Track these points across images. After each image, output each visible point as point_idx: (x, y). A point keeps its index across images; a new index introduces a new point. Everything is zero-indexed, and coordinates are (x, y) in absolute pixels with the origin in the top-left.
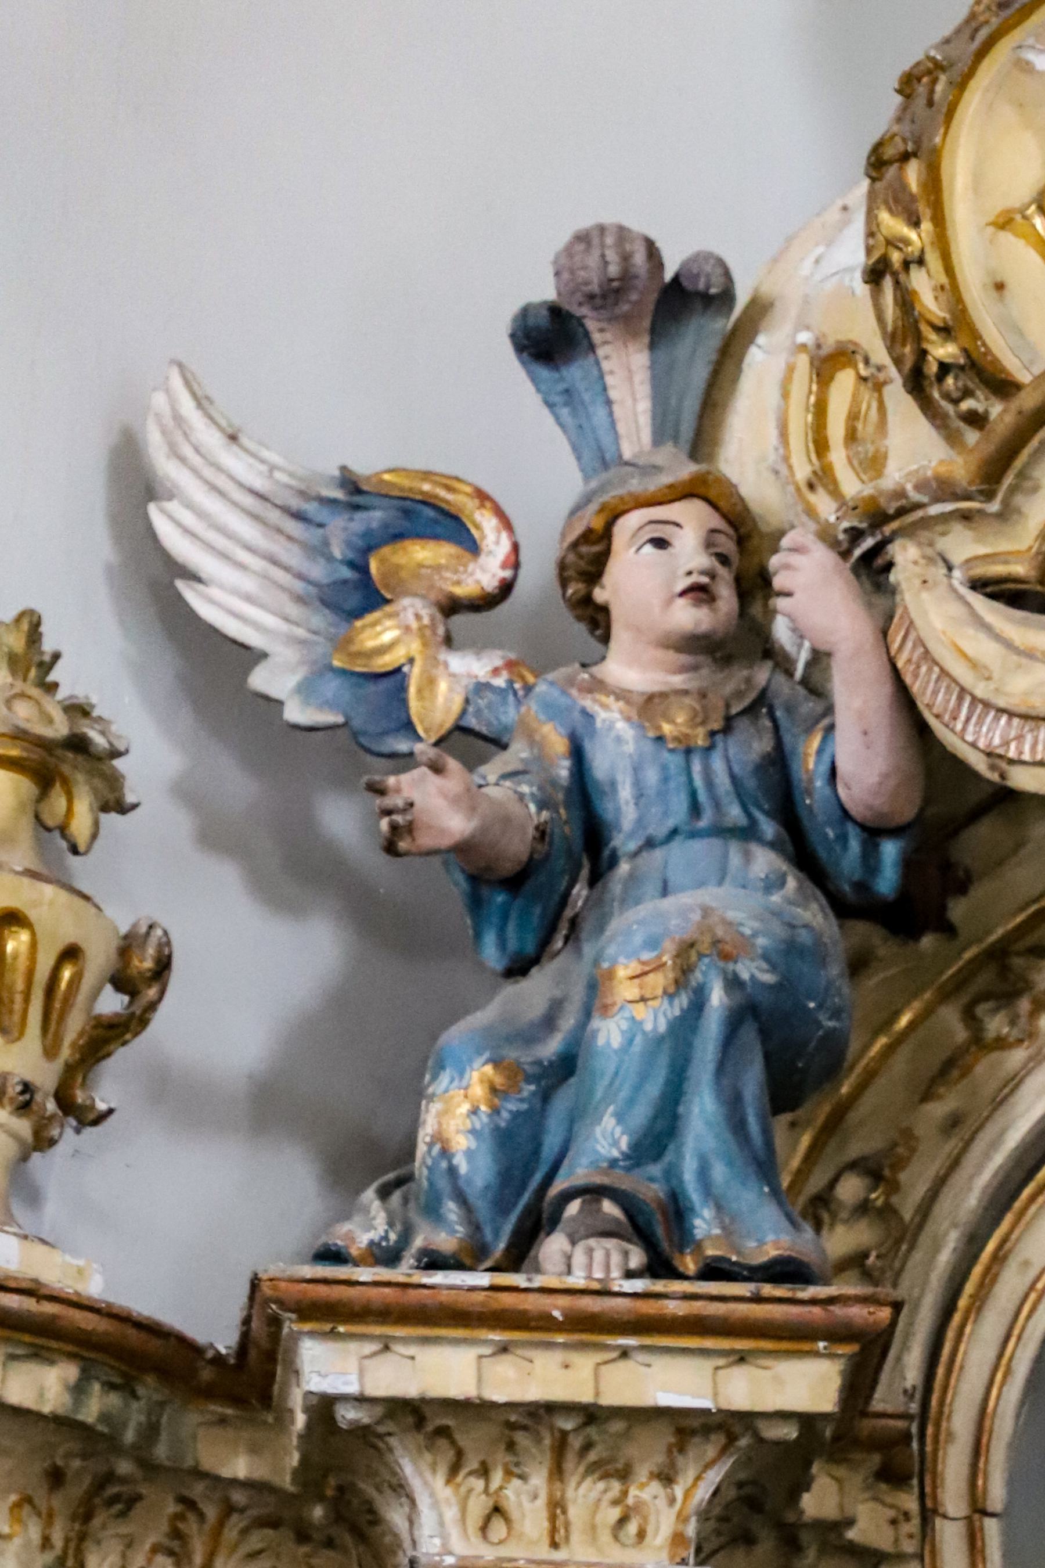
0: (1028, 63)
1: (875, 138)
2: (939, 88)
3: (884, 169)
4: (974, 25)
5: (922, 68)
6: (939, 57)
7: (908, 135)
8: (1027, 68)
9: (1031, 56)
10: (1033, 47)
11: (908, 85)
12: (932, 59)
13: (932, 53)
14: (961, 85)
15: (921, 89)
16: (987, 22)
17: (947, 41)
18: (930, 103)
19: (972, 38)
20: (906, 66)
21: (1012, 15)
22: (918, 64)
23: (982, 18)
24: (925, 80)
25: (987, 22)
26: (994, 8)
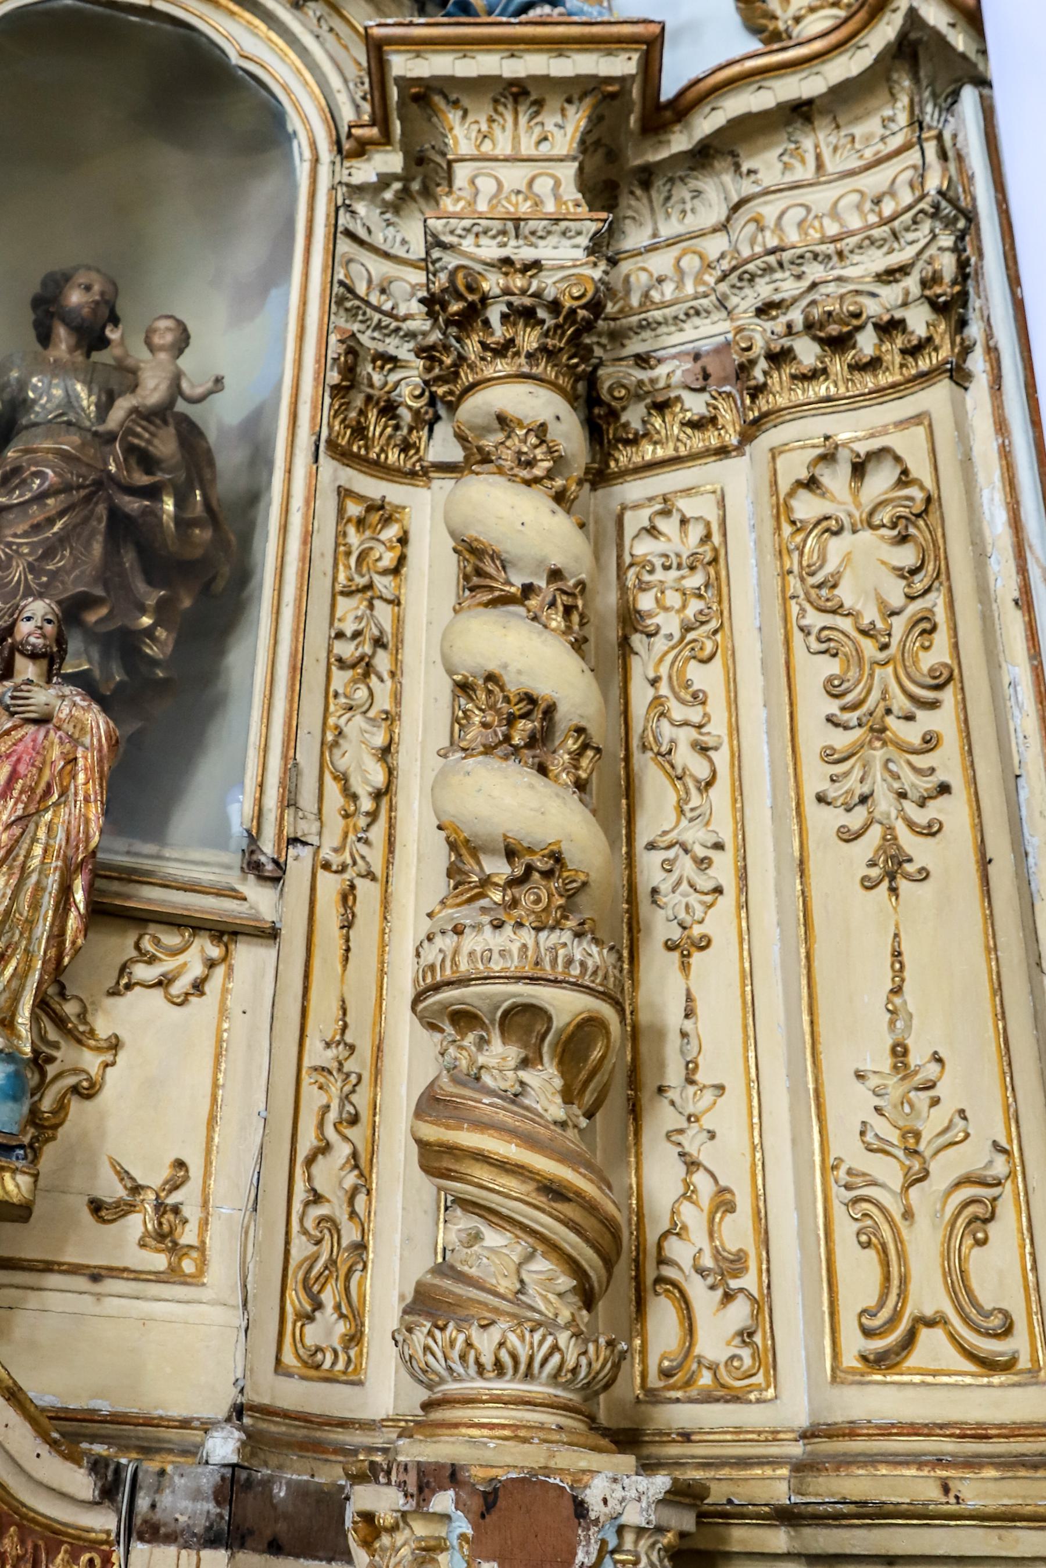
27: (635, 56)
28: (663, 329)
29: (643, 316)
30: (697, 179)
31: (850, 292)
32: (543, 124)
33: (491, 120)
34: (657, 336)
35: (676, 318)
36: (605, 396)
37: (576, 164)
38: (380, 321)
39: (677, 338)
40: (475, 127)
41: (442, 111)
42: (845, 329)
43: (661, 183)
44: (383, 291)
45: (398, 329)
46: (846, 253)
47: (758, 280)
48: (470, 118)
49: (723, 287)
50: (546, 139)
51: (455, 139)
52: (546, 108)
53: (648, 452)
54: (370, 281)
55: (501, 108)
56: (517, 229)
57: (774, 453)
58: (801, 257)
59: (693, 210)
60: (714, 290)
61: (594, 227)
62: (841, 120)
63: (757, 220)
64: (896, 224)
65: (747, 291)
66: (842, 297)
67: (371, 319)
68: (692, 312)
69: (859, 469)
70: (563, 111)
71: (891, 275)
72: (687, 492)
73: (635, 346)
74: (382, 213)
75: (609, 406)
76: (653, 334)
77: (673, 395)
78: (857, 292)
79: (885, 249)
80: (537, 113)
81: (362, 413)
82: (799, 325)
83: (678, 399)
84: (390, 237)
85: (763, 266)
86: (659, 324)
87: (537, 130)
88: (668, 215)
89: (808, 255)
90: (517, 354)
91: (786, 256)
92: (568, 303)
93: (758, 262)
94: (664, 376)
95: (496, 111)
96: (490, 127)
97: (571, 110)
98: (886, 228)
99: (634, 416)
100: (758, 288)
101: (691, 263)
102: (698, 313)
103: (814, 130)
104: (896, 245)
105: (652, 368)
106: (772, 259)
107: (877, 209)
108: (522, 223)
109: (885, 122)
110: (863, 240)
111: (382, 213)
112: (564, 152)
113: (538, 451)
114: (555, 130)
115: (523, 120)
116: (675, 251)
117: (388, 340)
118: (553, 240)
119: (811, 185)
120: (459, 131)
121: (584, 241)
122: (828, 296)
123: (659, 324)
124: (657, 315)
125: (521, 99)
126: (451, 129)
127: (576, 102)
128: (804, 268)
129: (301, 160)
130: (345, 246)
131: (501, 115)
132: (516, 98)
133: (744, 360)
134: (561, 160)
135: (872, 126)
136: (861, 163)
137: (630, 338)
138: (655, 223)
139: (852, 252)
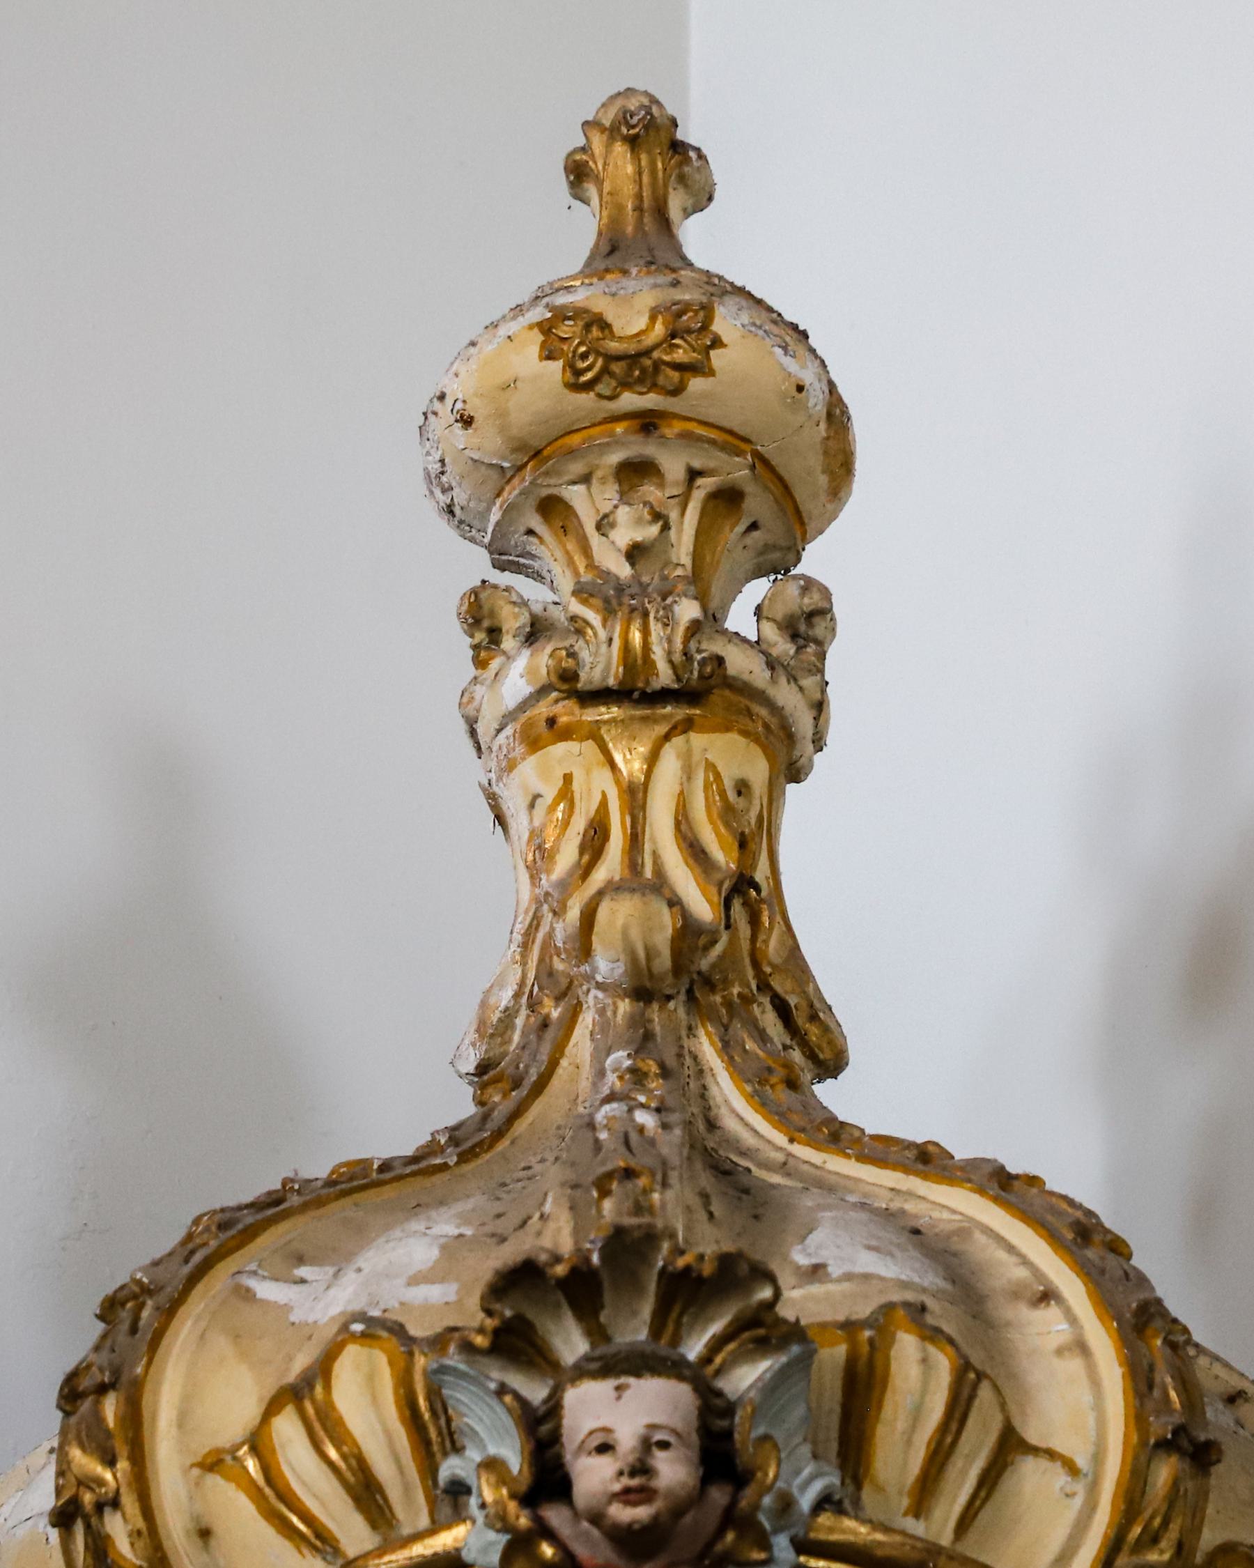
0: (248, 1290)
1: (69, 1366)
2: (145, 1314)
3: (79, 1402)
4: (190, 1246)
5: (125, 1292)
6: (145, 1280)
7: (105, 1364)
8: (247, 1295)
9: (252, 1283)
10: (255, 1273)
11: (110, 1309)
12: (139, 1283)
13: (139, 1276)
14: (169, 1312)
15: (125, 1315)
16: (205, 1244)
17: (156, 1263)
18: (134, 1330)
19: (186, 1261)
20: (110, 1289)
21: (233, 1237)
22: (122, 1287)
23: (198, 1241)
24: (129, 1305)
25: (205, 1244)
26: (214, 1228)
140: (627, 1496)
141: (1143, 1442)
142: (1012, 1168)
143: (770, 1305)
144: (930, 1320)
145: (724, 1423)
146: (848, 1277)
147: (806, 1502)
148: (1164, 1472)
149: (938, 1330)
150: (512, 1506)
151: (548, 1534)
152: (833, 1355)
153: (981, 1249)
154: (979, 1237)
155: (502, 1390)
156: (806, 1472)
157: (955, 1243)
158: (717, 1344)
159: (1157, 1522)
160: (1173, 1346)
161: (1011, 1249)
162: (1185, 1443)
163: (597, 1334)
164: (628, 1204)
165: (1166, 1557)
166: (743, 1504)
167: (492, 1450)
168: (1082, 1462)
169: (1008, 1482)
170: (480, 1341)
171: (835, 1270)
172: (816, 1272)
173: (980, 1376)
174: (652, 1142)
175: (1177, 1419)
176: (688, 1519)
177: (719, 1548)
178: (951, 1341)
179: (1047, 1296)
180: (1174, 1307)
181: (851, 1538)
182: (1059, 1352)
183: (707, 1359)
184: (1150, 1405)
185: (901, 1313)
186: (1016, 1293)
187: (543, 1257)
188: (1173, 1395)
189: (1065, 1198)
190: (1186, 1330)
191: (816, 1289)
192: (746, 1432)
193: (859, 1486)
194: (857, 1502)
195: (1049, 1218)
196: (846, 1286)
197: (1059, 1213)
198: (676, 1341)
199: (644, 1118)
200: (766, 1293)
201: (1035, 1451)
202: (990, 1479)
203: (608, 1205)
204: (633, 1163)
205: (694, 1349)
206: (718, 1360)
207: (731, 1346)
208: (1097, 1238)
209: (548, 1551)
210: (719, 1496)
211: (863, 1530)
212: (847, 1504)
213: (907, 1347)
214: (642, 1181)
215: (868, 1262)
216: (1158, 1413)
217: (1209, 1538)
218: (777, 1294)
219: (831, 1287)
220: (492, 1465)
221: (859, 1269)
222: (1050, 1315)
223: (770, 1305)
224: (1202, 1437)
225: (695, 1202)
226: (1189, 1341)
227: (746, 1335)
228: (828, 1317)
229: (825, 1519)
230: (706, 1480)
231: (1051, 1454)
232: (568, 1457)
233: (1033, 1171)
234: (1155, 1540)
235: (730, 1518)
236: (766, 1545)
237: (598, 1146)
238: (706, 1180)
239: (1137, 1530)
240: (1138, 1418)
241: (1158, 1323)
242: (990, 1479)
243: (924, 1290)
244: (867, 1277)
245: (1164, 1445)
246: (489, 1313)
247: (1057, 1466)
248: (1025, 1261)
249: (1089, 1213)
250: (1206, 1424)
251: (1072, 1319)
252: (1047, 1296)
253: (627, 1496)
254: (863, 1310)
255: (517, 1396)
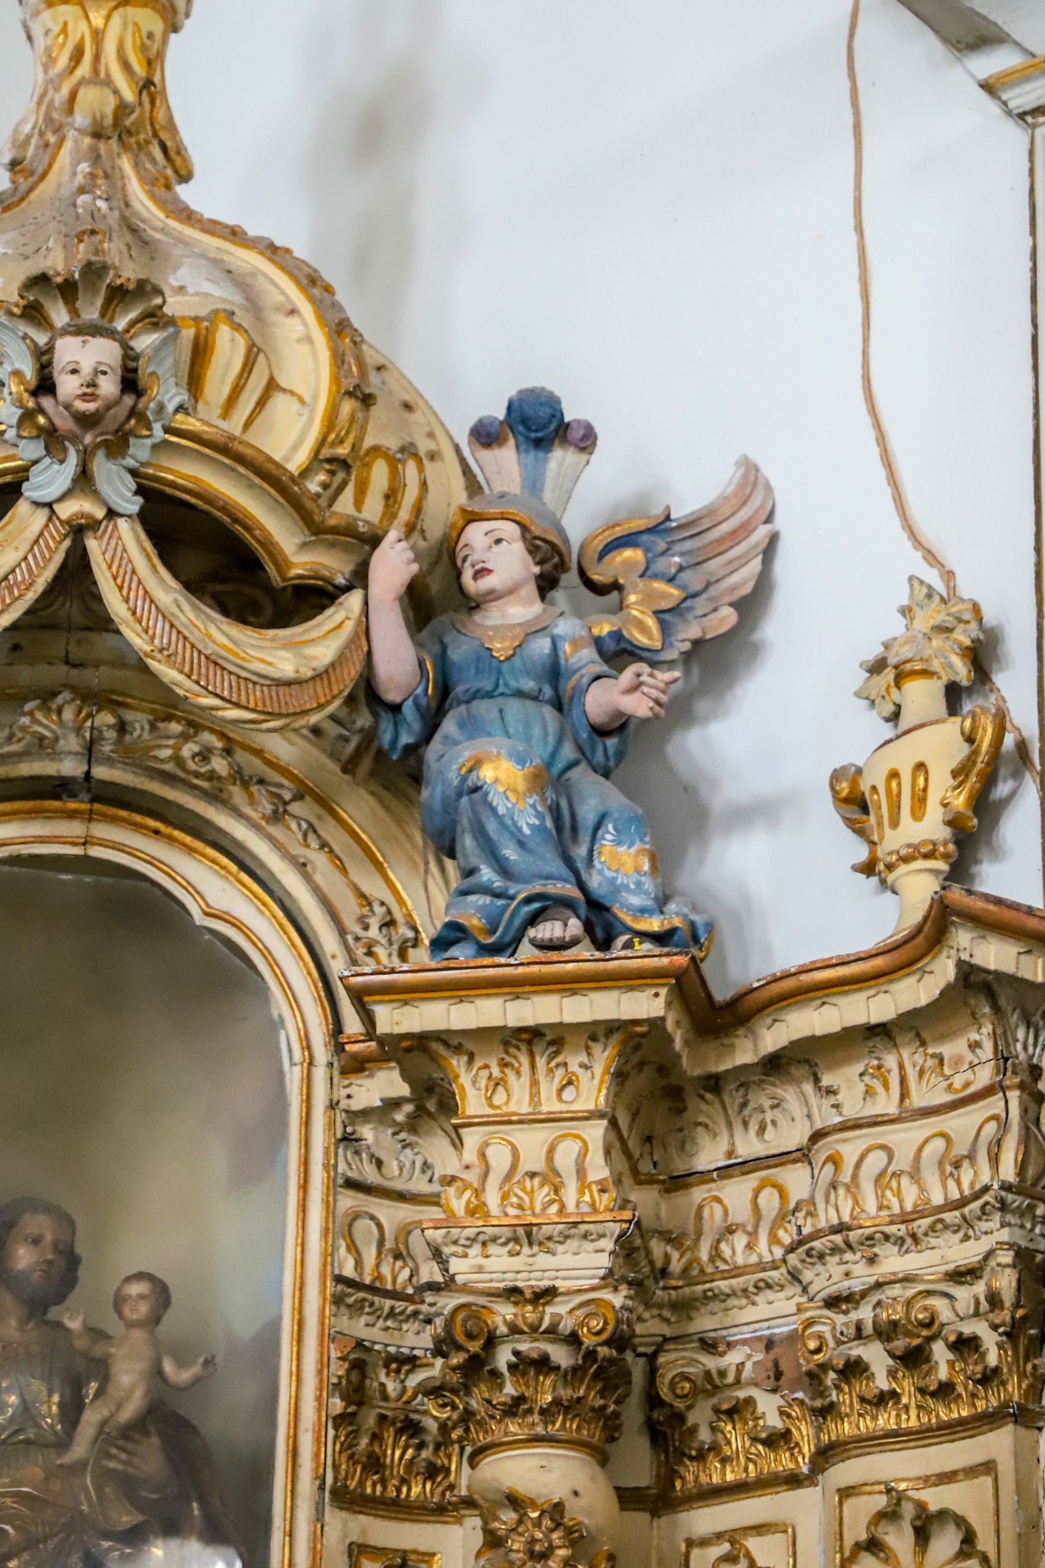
27: (663, 992)
28: (733, 1302)
29: (708, 1286)
30: (774, 1085)
31: (920, 1293)
32: (565, 1064)
33: (504, 1065)
34: (727, 1310)
35: (745, 1291)
36: (665, 1393)
37: (605, 1122)
38: (392, 1308)
39: (750, 1314)
40: (485, 1073)
41: (445, 1058)
42: (916, 1342)
43: (733, 1086)
44: (398, 1256)
45: (416, 1314)
46: (920, 1236)
47: (828, 1258)
48: (478, 1063)
49: (793, 1259)
50: (570, 1083)
51: (462, 1088)
52: (567, 1046)
53: (716, 1474)
54: (381, 1243)
55: (513, 1051)
56: (529, 1235)
57: (846, 1493)
58: (870, 1238)
59: (774, 1123)
60: (784, 1261)
61: (617, 1229)
62: (926, 1035)
63: (835, 1160)
64: (966, 1210)
65: (819, 1268)
66: (909, 1303)
67: (382, 1308)
68: (762, 1284)
69: (922, 1534)
70: (587, 1048)
71: (961, 1275)
72: (760, 1529)
73: (704, 1323)
74: (395, 1134)
75: (671, 1406)
76: (723, 1305)
77: (742, 1394)
78: (929, 1293)
79: (961, 1234)
80: (557, 1053)
81: (376, 1437)
82: (868, 1329)
83: (750, 1401)
84: (408, 1164)
85: (829, 1245)
86: (728, 1296)
87: (560, 1072)
88: (745, 1124)
89: (878, 1236)
90: (530, 1411)
91: (854, 1236)
92: (588, 1341)
93: (823, 1240)
94: (733, 1368)
95: (507, 1053)
96: (502, 1072)
97: (597, 1048)
98: (957, 1213)
99: (700, 1416)
100: (829, 1266)
101: (769, 1200)
102: (769, 1286)
103: (896, 1045)
104: (971, 1232)
105: (722, 1354)
106: (838, 1238)
107: (955, 1172)
108: (535, 1229)
109: (974, 1046)
110: (935, 1223)
111: (395, 1134)
112: (591, 1106)
113: (555, 1536)
114: (581, 1072)
115: (541, 1062)
116: (752, 1181)
117: (405, 1327)
118: (572, 1244)
119: (892, 1121)
120: (465, 1079)
121: (608, 1244)
122: (894, 1299)
123: (728, 1296)
124: (723, 1285)
125: (535, 1041)
126: (457, 1077)
127: (603, 1039)
128: (876, 1250)
129: (293, 1064)
130: (348, 1201)
131: (515, 1057)
132: (529, 1043)
133: (812, 1366)
134: (587, 1119)
135: (954, 1048)
136: (947, 1098)
137: (697, 1309)
138: (732, 1136)
139: (926, 1234)
140: (84, 398)
141: (338, 392)
142: (278, 243)
143: (160, 307)
144: (236, 319)
145: (134, 364)
146: (197, 294)
147: (171, 407)
148: (347, 407)
149: (240, 325)
150: (26, 395)
151: (41, 411)
152: (188, 333)
153: (261, 284)
154: (260, 277)
155: (25, 337)
156: (173, 392)
157: (249, 280)
158: (133, 323)
159: (343, 433)
160: (355, 343)
161: (276, 285)
162: (359, 394)
163: (74, 313)
164: (92, 248)
165: (346, 451)
166: (140, 406)
167: (17, 366)
168: (307, 398)
169: (270, 405)
170: (16, 310)
171: (191, 290)
172: (181, 289)
173: (259, 350)
174: (105, 217)
175: (355, 381)
176: (112, 411)
177: (127, 427)
178: (246, 331)
179: (293, 312)
180: (356, 323)
181: (191, 428)
182: (299, 341)
183: (127, 331)
184: (342, 373)
185: (222, 315)
186: (278, 309)
187: (51, 272)
188: (354, 369)
189: (303, 262)
190: (361, 335)
191: (180, 299)
192: (145, 369)
193: (196, 401)
194: (195, 409)
195: (296, 272)
196: (196, 299)
197: (301, 270)
198: (111, 320)
199: (101, 204)
200: (158, 301)
201: (284, 390)
202: (262, 403)
203: (82, 246)
204: (95, 227)
205: (120, 324)
206: (132, 331)
207: (139, 325)
208: (319, 283)
209: (41, 420)
210: (129, 400)
211: (198, 424)
212: (190, 410)
213: (224, 334)
214: (99, 237)
215: (207, 287)
216: (346, 377)
217: (368, 442)
218: (164, 302)
219: (187, 298)
220: (16, 373)
221: (202, 290)
222: (294, 322)
223: (160, 307)
224: (367, 391)
225: (124, 248)
226: (363, 341)
227: (147, 321)
228: (186, 313)
229: (180, 417)
230: (123, 391)
231: (292, 393)
232: (55, 374)
233: (288, 245)
234: (342, 442)
235: (133, 413)
236: (150, 429)
237: (78, 217)
238: (129, 237)
239: (332, 436)
240: (336, 379)
241: (347, 331)
242: (262, 403)
243: (233, 304)
244: (206, 295)
245: (349, 394)
246: (22, 297)
247: (295, 399)
248: (283, 293)
249: (315, 271)
250: (368, 385)
251: (305, 324)
252: (293, 312)
253: (84, 398)
254: (203, 312)
255: (32, 340)
